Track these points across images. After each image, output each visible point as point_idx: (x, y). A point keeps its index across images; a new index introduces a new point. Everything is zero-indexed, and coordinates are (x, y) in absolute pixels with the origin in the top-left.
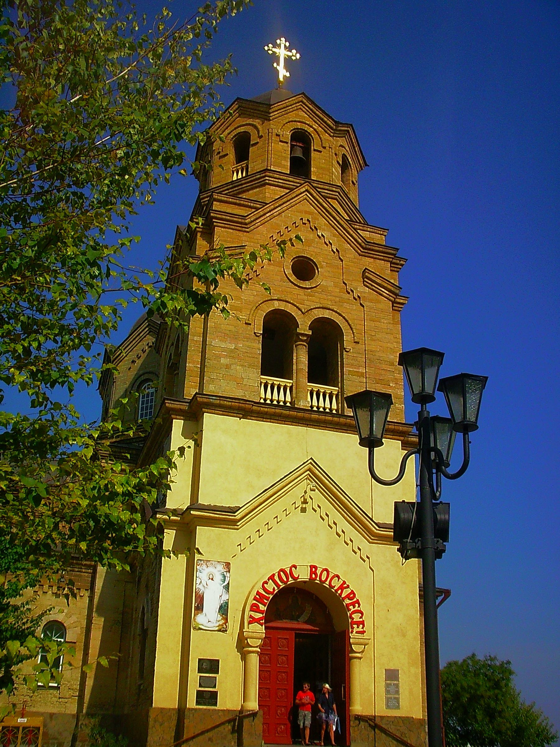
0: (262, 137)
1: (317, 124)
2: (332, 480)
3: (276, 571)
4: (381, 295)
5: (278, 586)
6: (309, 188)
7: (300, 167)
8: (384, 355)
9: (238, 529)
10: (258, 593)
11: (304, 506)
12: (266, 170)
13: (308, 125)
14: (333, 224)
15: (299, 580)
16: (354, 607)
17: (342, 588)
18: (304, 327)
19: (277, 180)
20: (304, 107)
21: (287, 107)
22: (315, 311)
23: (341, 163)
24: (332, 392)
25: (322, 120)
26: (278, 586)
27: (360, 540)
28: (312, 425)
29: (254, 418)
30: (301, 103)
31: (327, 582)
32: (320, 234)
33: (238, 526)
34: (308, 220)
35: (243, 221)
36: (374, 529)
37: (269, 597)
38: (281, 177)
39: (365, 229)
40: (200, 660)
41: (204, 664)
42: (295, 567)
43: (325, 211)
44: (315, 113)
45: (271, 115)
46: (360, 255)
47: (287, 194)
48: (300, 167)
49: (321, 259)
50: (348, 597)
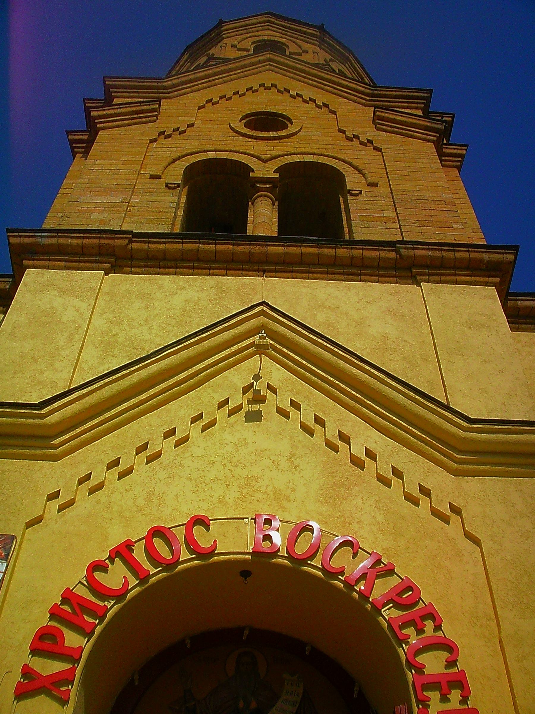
2: (321, 336)
4: (412, 137)
5: (143, 577)
9: (56, 458)
10: (68, 596)
11: (256, 407)
15: (215, 558)
16: (420, 631)
20: (273, 27)
26: (143, 577)
27: (419, 470)
28: (277, 271)
29: (138, 270)
31: (317, 562)
33: (56, 447)
35: (159, 84)
36: (455, 430)
37: (106, 610)
42: (201, 521)
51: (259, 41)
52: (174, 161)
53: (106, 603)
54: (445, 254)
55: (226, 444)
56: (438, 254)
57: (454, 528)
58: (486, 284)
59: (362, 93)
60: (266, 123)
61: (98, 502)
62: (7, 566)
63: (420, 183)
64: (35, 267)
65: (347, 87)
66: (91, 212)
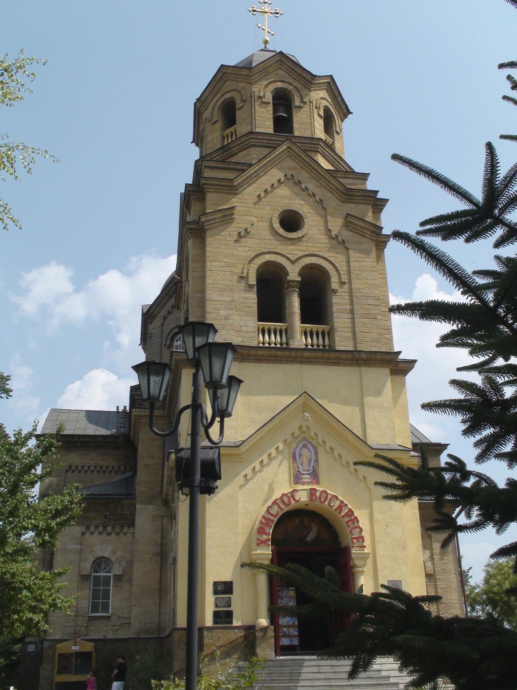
0: (245, 101)
1: (297, 80)
4: (364, 236)
6: (291, 146)
7: (283, 124)
12: (251, 133)
13: (289, 83)
14: (315, 176)
18: (294, 274)
19: (261, 141)
21: (267, 68)
22: (304, 259)
23: (323, 115)
24: (324, 330)
25: (301, 75)
26: (282, 509)
30: (279, 62)
31: (326, 503)
32: (303, 187)
34: (292, 176)
35: (231, 184)
38: (265, 138)
39: (347, 176)
40: (215, 584)
41: (219, 586)
43: (306, 165)
44: (293, 70)
45: (253, 77)
46: (342, 202)
47: (271, 152)
48: (283, 124)
50: (346, 514)
52: (250, 262)
59: (341, 192)
63: (366, 281)
65: (333, 185)
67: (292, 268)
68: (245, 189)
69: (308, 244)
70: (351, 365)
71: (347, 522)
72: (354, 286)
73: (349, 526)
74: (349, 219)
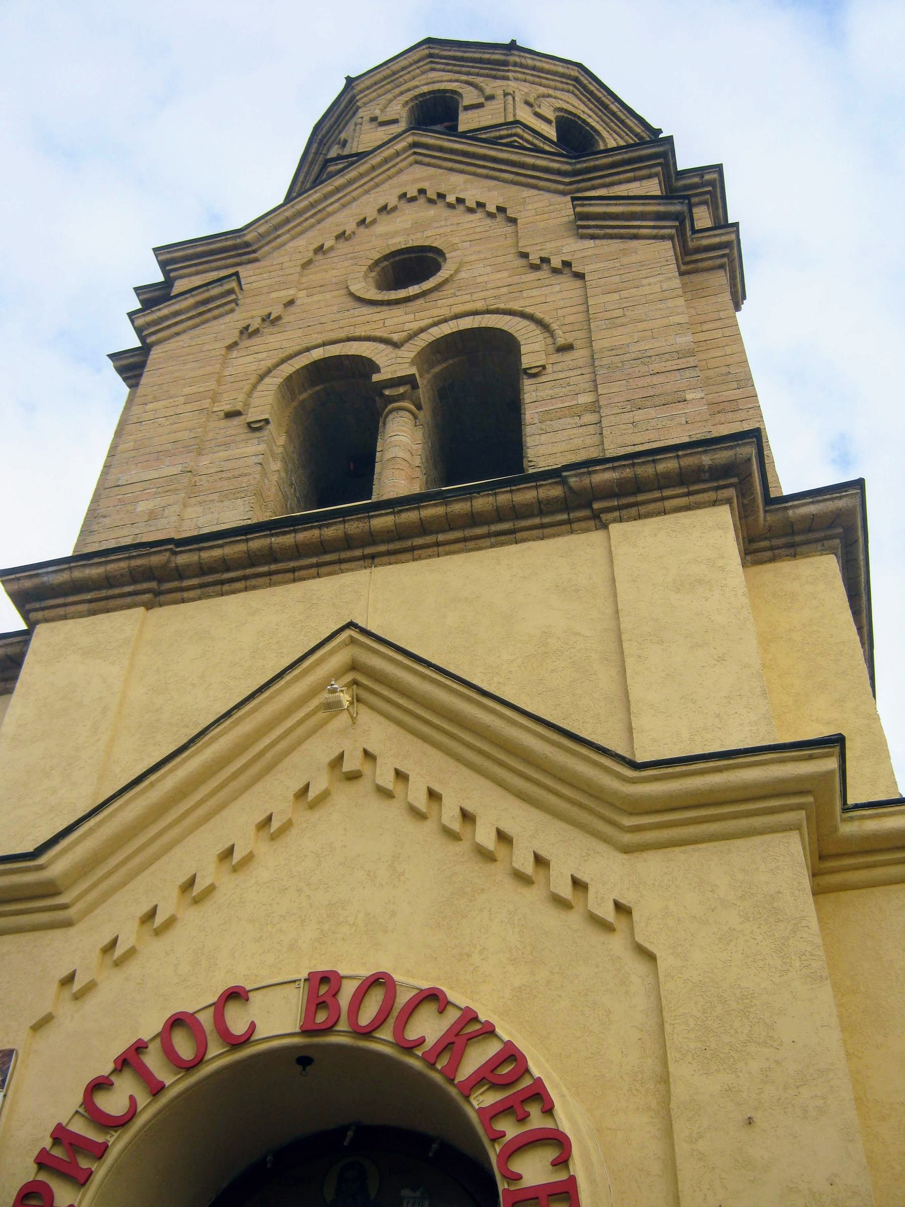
3: (150, 1026)
4: (635, 237)
5: (156, 1089)
8: (656, 345)
10: (60, 1135)
17: (455, 1042)
26: (156, 1089)
27: (573, 853)
35: (238, 241)
42: (235, 995)
49: (456, 240)
50: (486, 1077)
51: (416, 97)
52: (262, 377)
53: (108, 1138)
54: (640, 470)
55: (306, 856)
56: (628, 473)
57: (617, 943)
58: (715, 503)
60: (411, 268)
61: (127, 979)
62: (5, 1096)
63: (641, 326)
64: (47, 620)
65: (534, 168)
66: (135, 502)
67: (394, 355)
68: (284, 244)
69: (451, 301)
70: (569, 527)
71: (492, 1114)
72: (596, 346)
73: (497, 1137)
74: (578, 209)
